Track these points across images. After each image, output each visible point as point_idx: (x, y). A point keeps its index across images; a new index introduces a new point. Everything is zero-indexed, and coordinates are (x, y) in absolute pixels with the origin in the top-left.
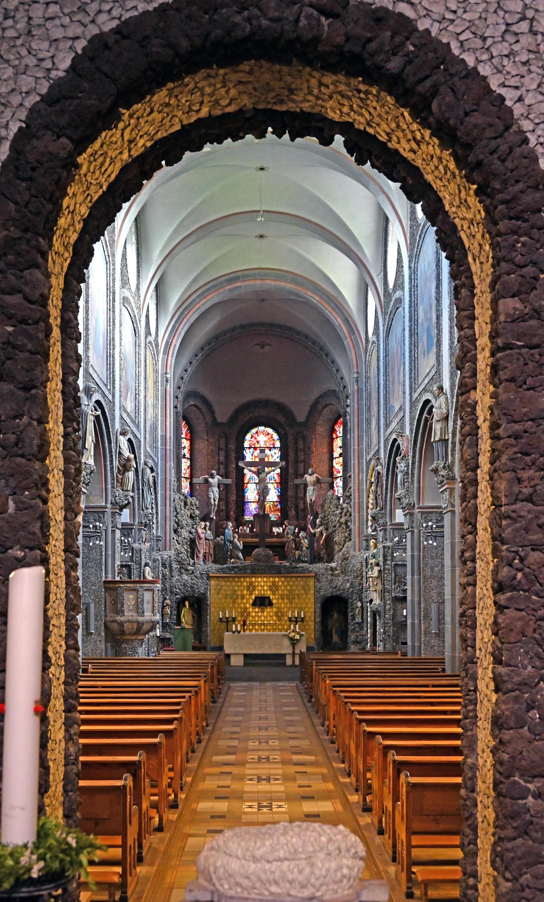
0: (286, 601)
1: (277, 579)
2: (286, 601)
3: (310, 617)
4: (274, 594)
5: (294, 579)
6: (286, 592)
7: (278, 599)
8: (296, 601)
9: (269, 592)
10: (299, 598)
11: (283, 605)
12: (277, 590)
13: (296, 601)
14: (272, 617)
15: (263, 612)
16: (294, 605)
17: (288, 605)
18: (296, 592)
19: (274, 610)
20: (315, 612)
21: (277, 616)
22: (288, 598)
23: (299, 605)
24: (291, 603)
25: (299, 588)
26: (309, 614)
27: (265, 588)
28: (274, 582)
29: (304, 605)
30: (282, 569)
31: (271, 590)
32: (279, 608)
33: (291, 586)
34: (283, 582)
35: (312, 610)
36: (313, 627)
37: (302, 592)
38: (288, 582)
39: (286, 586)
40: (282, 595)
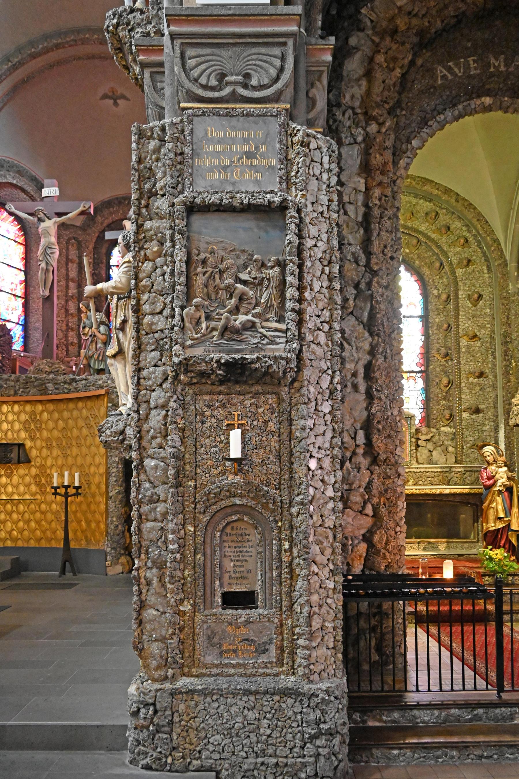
0: (56, 452)
1: (40, 407)
2: (56, 452)
3: (98, 486)
4: (32, 439)
5: (71, 405)
6: (56, 433)
7: (40, 450)
8: (75, 451)
9: (23, 435)
10: (79, 446)
11: (49, 462)
12: (40, 430)
13: (75, 451)
14: (28, 486)
15: (9, 476)
16: (70, 461)
17: (60, 462)
18: (75, 432)
19: (34, 471)
20: (108, 474)
21: (38, 484)
22: (59, 446)
23: (79, 461)
24: (66, 456)
25: (81, 423)
26: (97, 479)
27: (17, 426)
28: (33, 413)
29: (89, 459)
30: (50, 386)
31: (26, 430)
32: (42, 467)
33: (66, 421)
34: (51, 413)
35: (102, 470)
36: (103, 507)
37: (85, 431)
38: (60, 412)
39: (56, 422)
40: (48, 439)
